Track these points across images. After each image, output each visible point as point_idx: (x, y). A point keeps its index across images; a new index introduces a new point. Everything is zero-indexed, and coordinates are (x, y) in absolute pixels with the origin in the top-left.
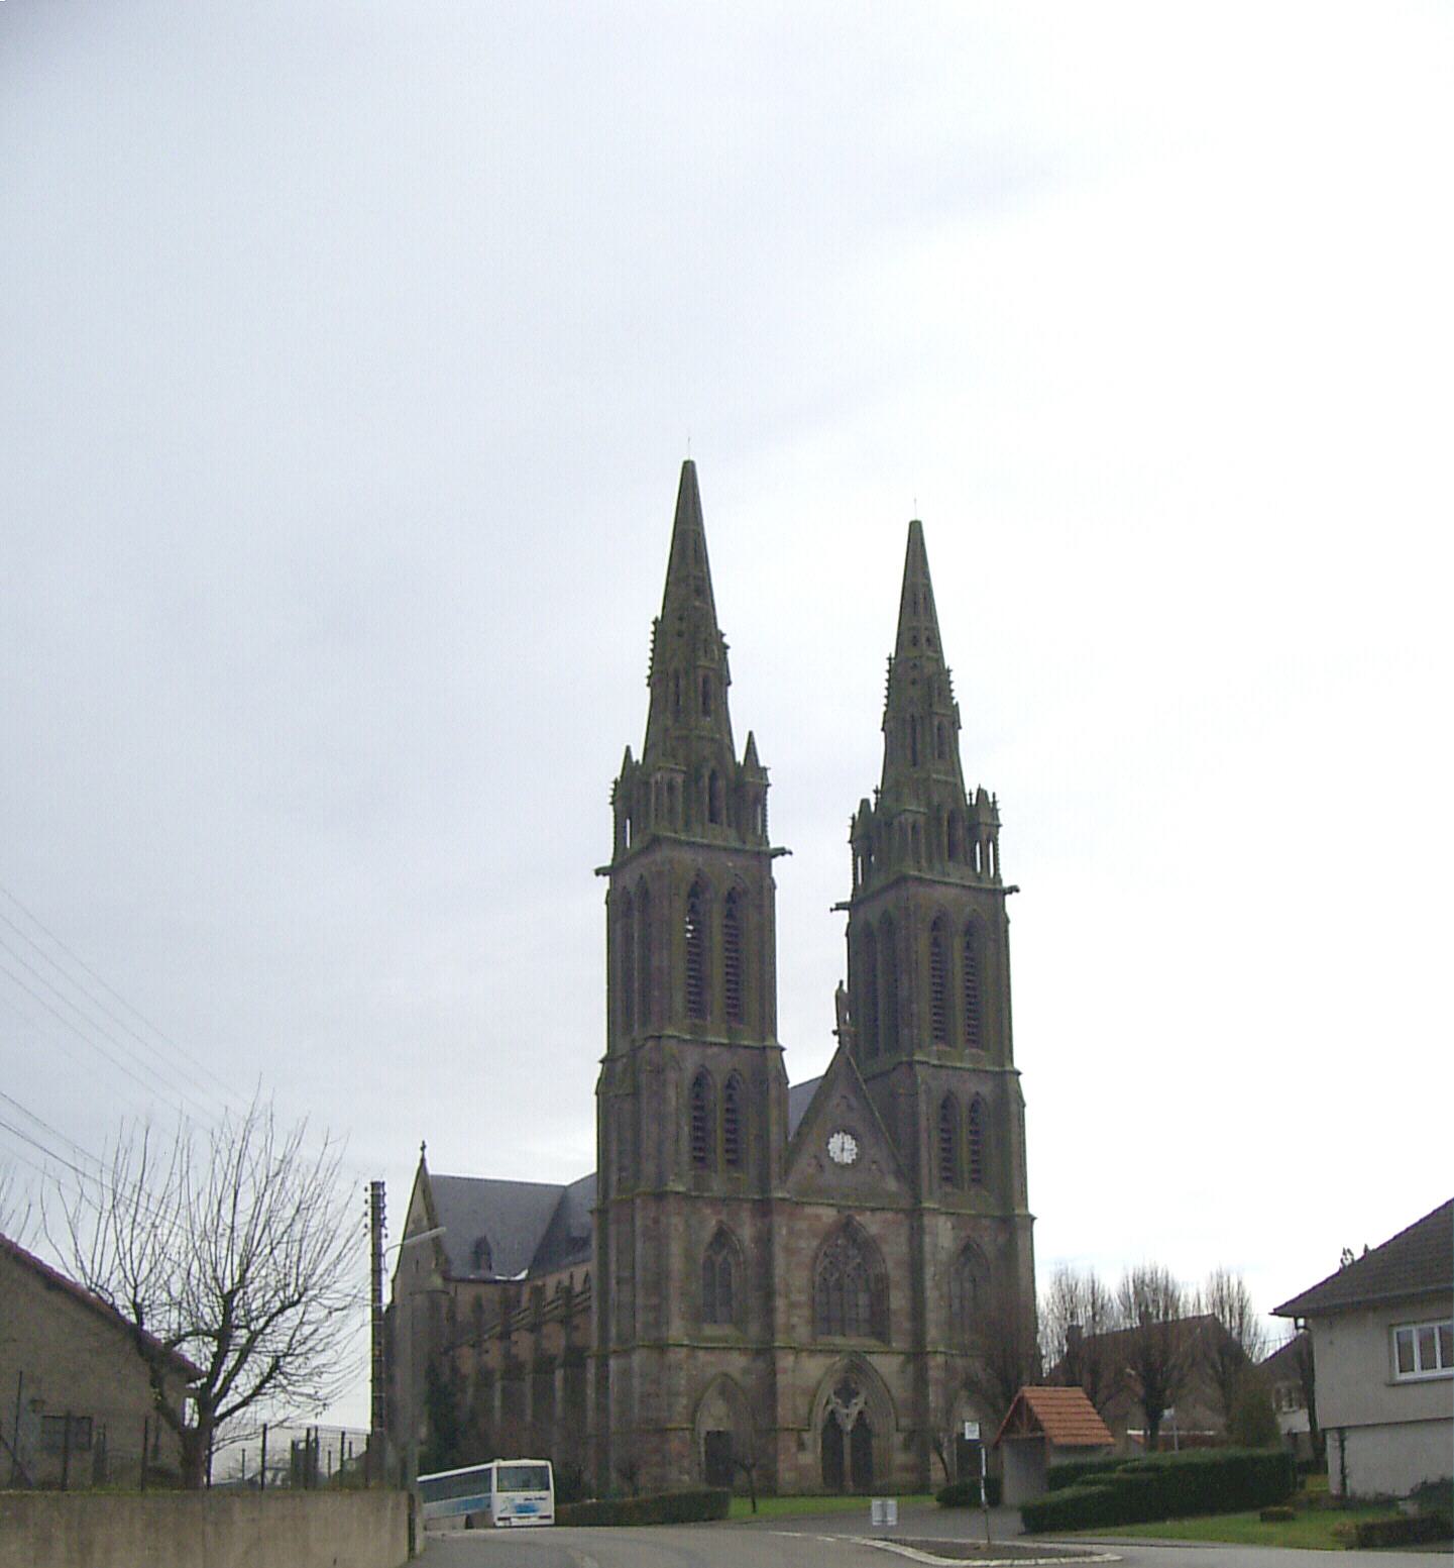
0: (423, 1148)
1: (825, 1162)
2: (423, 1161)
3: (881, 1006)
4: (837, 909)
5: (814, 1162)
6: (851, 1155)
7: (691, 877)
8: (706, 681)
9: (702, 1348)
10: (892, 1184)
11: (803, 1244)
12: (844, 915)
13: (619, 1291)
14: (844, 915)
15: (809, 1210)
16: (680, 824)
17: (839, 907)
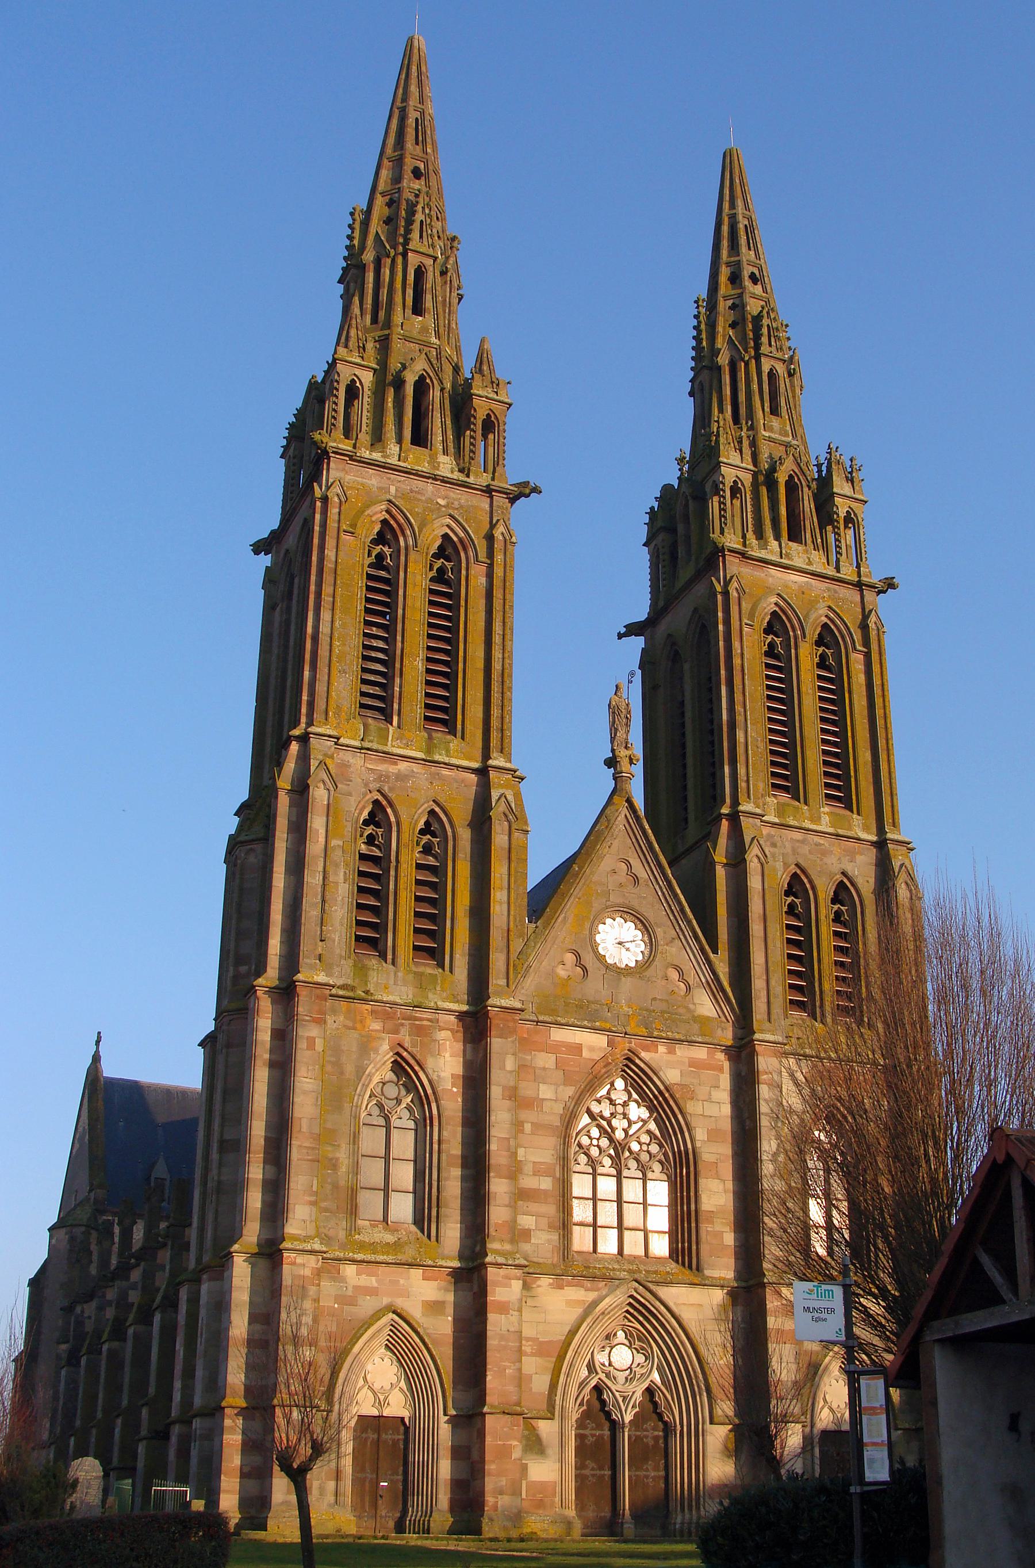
0: (98, 1042)
1: (588, 959)
2: (96, 1058)
3: (688, 715)
4: (626, 634)
5: (570, 958)
6: (637, 946)
7: (378, 512)
8: (420, 272)
9: (354, 1261)
10: (705, 1005)
11: (546, 1092)
12: (638, 643)
13: (220, 1165)
14: (638, 643)
15: (559, 1035)
16: (364, 437)
17: (633, 630)
